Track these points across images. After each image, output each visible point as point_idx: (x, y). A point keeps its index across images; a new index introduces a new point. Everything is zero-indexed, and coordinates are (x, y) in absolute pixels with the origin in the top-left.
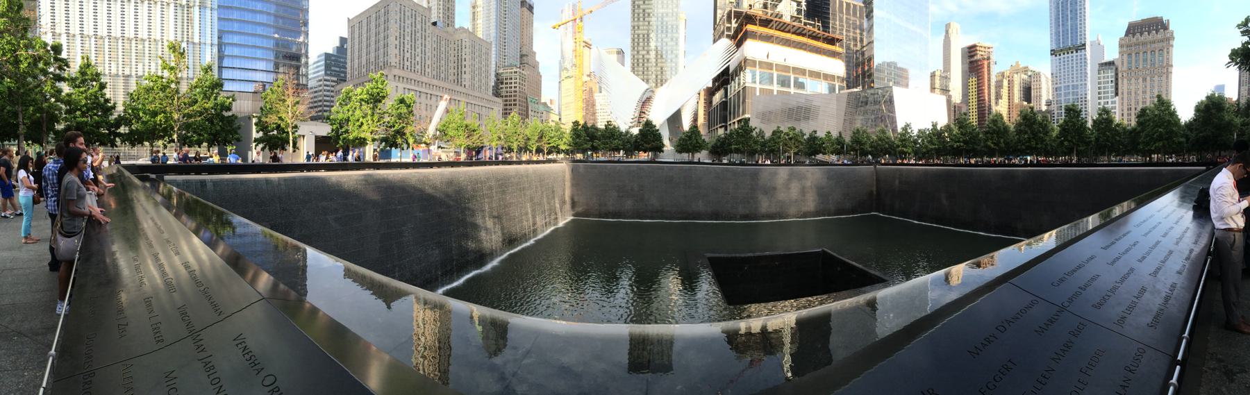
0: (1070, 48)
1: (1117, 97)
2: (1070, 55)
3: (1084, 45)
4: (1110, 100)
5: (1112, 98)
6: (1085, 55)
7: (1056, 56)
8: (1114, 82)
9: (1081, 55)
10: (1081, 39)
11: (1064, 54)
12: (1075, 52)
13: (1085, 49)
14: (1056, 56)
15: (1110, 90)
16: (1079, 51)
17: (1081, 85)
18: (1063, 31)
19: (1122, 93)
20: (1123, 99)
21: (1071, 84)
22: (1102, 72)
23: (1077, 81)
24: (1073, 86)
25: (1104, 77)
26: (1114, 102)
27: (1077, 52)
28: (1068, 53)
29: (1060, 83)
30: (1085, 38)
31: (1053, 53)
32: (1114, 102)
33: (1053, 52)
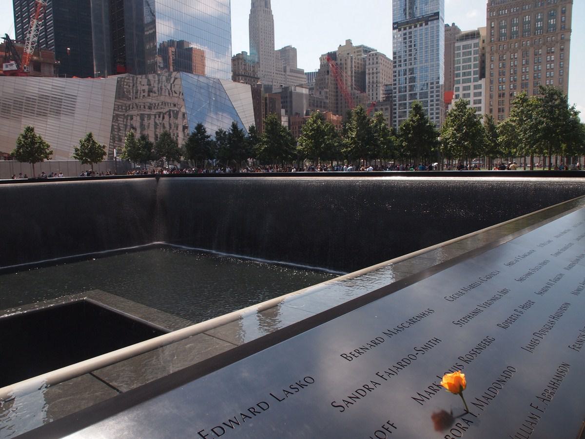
1: (482, 79)
4: (472, 85)
5: (475, 80)
6: (438, 27)
7: (400, 30)
12: (424, 24)
13: (438, 19)
16: (429, 23)
17: (432, 66)
20: (491, 82)
23: (426, 61)
27: (427, 24)
32: (480, 86)
33: (396, 26)
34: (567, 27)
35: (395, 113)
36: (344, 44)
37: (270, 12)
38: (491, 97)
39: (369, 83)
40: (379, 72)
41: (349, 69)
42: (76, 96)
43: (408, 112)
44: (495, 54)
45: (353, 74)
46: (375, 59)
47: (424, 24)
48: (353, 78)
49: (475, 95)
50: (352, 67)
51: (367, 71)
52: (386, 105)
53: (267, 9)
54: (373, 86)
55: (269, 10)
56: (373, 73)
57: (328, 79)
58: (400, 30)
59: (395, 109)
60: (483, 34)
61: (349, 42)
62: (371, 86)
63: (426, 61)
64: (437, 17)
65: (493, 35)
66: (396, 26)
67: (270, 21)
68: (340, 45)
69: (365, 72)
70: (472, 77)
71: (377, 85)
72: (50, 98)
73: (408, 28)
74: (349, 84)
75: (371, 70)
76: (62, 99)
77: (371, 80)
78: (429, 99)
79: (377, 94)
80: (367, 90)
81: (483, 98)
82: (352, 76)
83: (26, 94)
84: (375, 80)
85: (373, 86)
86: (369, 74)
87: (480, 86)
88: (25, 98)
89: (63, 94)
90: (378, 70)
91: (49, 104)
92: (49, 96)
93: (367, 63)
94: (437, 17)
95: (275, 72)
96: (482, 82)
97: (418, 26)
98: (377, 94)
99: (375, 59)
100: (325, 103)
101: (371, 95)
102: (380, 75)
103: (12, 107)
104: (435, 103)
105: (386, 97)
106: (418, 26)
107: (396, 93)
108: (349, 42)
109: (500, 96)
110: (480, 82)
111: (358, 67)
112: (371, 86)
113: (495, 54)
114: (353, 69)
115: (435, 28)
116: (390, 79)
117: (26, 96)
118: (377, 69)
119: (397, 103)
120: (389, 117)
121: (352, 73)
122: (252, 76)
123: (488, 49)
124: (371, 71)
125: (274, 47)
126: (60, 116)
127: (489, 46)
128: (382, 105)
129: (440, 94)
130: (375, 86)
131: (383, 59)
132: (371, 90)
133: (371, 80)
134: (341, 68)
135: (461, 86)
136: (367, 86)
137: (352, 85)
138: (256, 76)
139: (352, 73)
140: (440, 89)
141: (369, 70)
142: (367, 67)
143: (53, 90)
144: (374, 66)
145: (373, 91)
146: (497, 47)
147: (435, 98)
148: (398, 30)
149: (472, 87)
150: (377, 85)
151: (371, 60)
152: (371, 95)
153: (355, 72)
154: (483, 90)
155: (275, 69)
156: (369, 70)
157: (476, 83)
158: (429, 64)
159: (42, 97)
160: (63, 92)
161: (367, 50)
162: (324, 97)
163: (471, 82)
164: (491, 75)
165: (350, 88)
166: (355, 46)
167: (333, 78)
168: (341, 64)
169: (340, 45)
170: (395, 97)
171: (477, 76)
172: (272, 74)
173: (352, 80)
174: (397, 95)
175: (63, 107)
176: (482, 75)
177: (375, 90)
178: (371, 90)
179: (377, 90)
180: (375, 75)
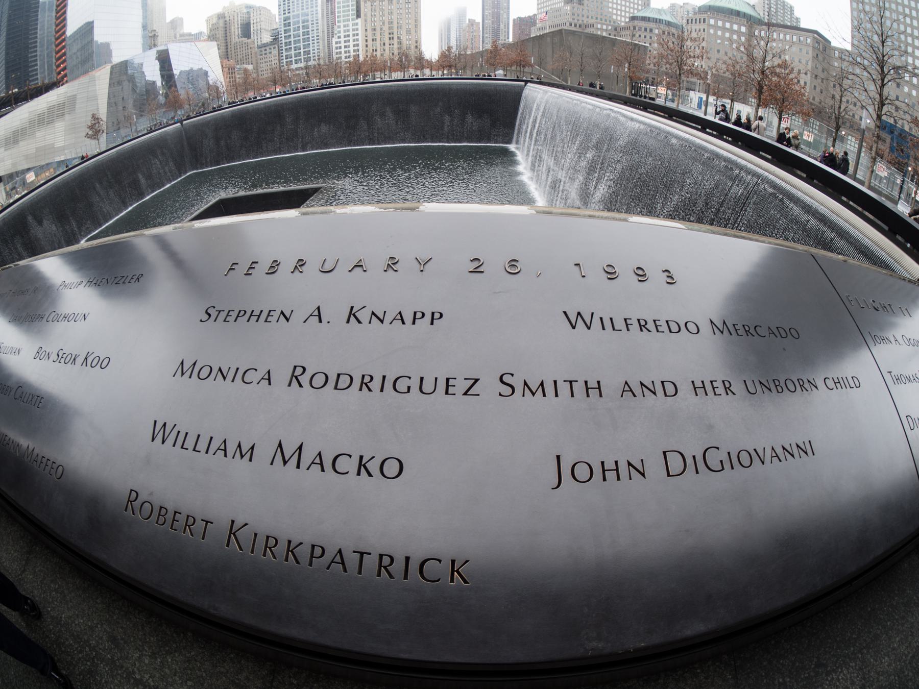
1: (359, 19)
4: (350, 23)
5: (353, 20)
15: (351, 12)
19: (365, 15)
20: (366, 21)
21: (300, 12)
23: (307, 8)
26: (357, 24)
29: (289, 13)
32: (357, 24)
39: (254, 30)
41: (236, 23)
43: (293, 48)
45: (239, 26)
48: (240, 29)
50: (238, 21)
51: (252, 22)
52: (274, 44)
56: (257, 23)
57: (219, 34)
59: (282, 47)
62: (255, 33)
63: (307, 8)
69: (250, 23)
70: (351, 17)
71: (261, 32)
74: (237, 34)
77: (255, 28)
80: (252, 36)
90: (262, 19)
93: (252, 16)
96: (359, 21)
101: (256, 39)
102: (262, 23)
105: (273, 39)
107: (282, 34)
110: (357, 21)
111: (243, 20)
112: (255, 33)
118: (260, 19)
120: (277, 55)
121: (238, 25)
124: (255, 21)
128: (271, 45)
132: (255, 36)
133: (255, 28)
134: (230, 23)
135: (342, 24)
136: (252, 33)
139: (238, 25)
140: (319, 28)
145: (257, 36)
150: (261, 32)
151: (255, 13)
152: (256, 39)
153: (241, 25)
154: (359, 27)
164: (365, 15)
165: (237, 37)
167: (223, 32)
168: (229, 20)
170: (281, 37)
171: (355, 17)
173: (238, 31)
174: (283, 35)
177: (259, 35)
178: (255, 36)
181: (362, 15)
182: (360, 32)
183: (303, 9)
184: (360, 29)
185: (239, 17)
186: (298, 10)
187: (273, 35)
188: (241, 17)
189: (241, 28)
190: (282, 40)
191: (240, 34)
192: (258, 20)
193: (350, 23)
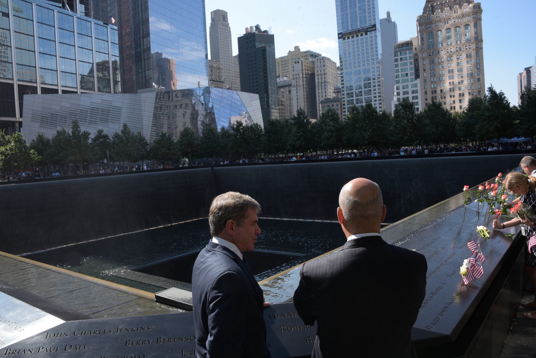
0: (359, 31)
1: (418, 80)
2: (360, 37)
3: (374, 26)
4: (410, 84)
6: (376, 36)
8: (413, 63)
9: (371, 37)
10: (370, 20)
11: (353, 37)
12: (364, 34)
13: (376, 30)
14: (344, 39)
16: (368, 33)
17: (373, 68)
18: (351, 13)
20: (425, 81)
22: (399, 53)
24: (364, 70)
25: (401, 59)
26: (416, 85)
27: (366, 34)
28: (357, 36)
30: (375, 19)
31: (341, 36)
33: (340, 36)
34: (479, 38)
35: (344, 108)
36: (292, 50)
37: (227, 25)
38: (426, 93)
39: (318, 83)
40: (326, 74)
42: (121, 107)
44: (426, 59)
46: (322, 63)
47: (364, 34)
48: (305, 79)
49: (413, 92)
51: (316, 73)
53: (225, 22)
54: (321, 85)
55: (226, 23)
58: (344, 39)
60: (416, 44)
61: (297, 48)
62: (320, 86)
64: (374, 28)
65: (423, 44)
66: (340, 36)
67: (228, 33)
68: (290, 51)
69: (314, 73)
71: (325, 84)
72: (100, 110)
73: (351, 37)
75: (319, 71)
76: (110, 110)
78: (373, 96)
79: (325, 92)
81: (419, 94)
82: (303, 78)
83: (80, 107)
84: (323, 81)
85: (321, 85)
86: (318, 75)
87: (416, 85)
88: (79, 111)
89: (110, 106)
91: (99, 114)
92: (99, 108)
93: (316, 66)
94: (374, 28)
95: (234, 75)
96: (418, 81)
97: (359, 35)
98: (325, 92)
99: (322, 63)
100: (282, 101)
103: (68, 118)
104: (377, 99)
106: (359, 35)
108: (297, 48)
109: (432, 93)
110: (416, 82)
112: (320, 86)
113: (426, 59)
114: (304, 71)
115: (373, 37)
116: (335, 79)
117: (80, 109)
118: (324, 70)
119: (346, 99)
122: (218, 80)
123: (420, 56)
125: (232, 54)
126: (108, 123)
127: (421, 53)
129: (381, 91)
130: (323, 85)
131: (329, 62)
132: (320, 89)
136: (317, 86)
137: (303, 85)
138: (221, 80)
139: (303, 74)
141: (318, 72)
142: (315, 69)
143: (103, 103)
144: (322, 68)
145: (322, 89)
146: (427, 54)
147: (377, 95)
148: (342, 39)
149: (410, 86)
150: (325, 84)
154: (419, 88)
155: (233, 73)
156: (318, 72)
157: (413, 83)
158: (371, 66)
159: (93, 109)
160: (110, 105)
161: (314, 55)
162: (281, 96)
163: (408, 82)
166: (302, 51)
169: (290, 51)
171: (414, 77)
172: (231, 77)
173: (303, 81)
175: (110, 116)
176: (417, 76)
177: (323, 89)
178: (320, 89)
179: (325, 89)
180: (323, 76)
181: (421, 75)
182: (419, 94)
183: (364, 65)
184: (419, 91)
185: (304, 65)
186: (359, 66)
187: (336, 91)
188: (305, 66)
189: (306, 78)
190: (344, 98)
191: (305, 84)
192: (323, 72)
193: (410, 84)
